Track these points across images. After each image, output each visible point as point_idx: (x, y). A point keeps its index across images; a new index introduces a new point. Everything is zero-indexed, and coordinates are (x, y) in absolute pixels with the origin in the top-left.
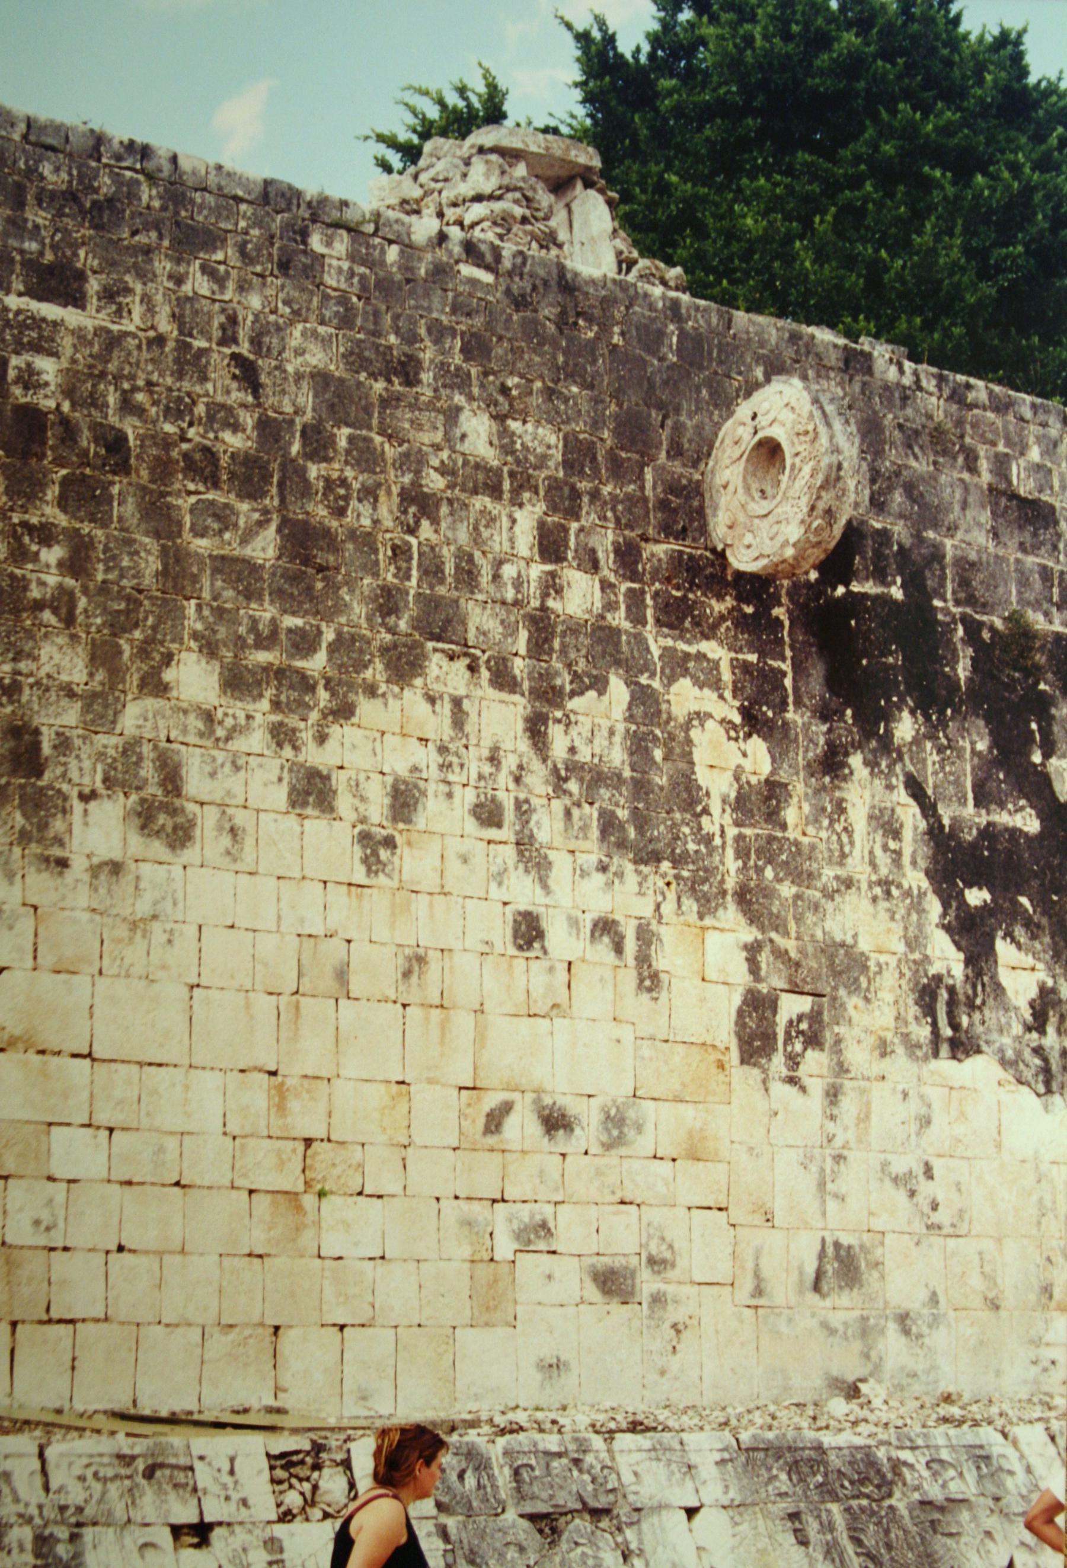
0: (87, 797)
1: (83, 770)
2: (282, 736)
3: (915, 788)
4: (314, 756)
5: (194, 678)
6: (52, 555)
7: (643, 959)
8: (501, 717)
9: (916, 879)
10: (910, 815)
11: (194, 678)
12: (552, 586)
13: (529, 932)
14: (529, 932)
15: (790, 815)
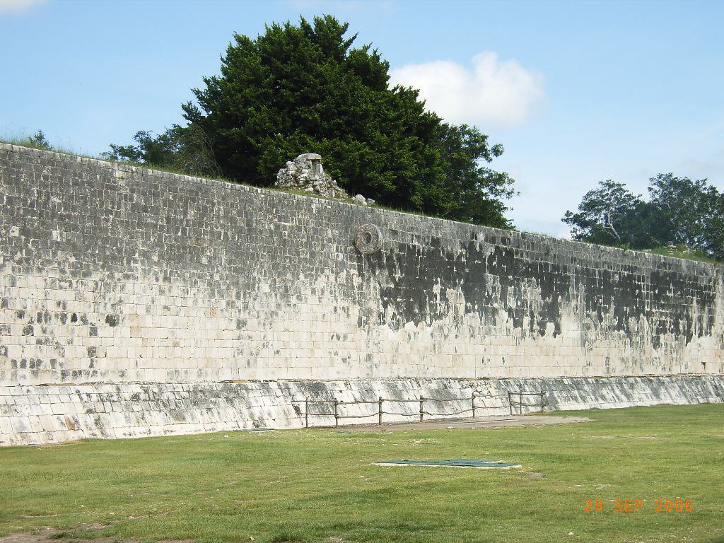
0: (292, 295)
1: (292, 292)
2: (311, 284)
3: (379, 282)
4: (314, 286)
5: (302, 276)
6: (288, 261)
7: (348, 312)
8: (332, 277)
9: (378, 297)
10: (378, 286)
11: (302, 276)
12: (338, 256)
13: (335, 310)
14: (335, 310)
15: (364, 289)
